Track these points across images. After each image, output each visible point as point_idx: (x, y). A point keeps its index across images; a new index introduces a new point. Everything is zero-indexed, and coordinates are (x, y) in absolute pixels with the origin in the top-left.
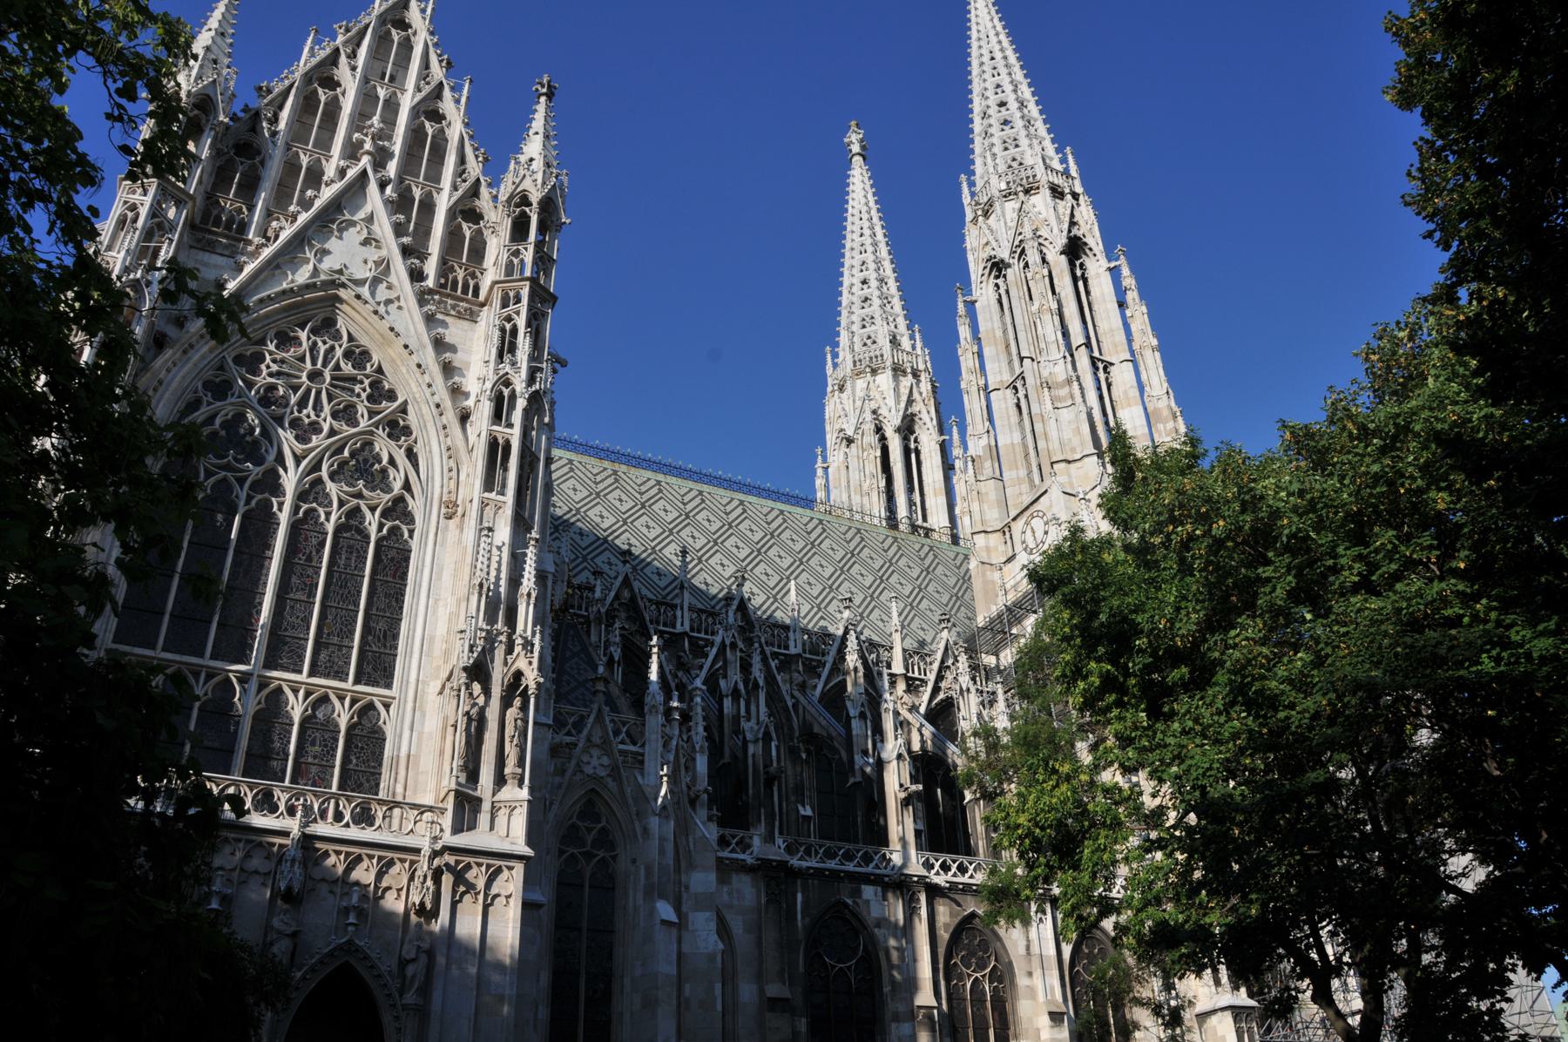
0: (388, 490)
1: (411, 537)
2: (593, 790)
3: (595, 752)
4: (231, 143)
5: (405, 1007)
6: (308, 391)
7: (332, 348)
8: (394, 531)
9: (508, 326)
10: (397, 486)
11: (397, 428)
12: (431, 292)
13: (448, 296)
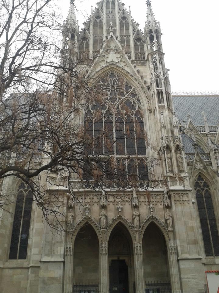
0: (135, 109)
1: (143, 119)
2: (200, 173)
3: (198, 163)
4: (81, 38)
5: (169, 231)
6: (112, 91)
8: (139, 118)
9: (154, 64)
10: (137, 108)
11: (134, 95)
12: (134, 61)
13: (138, 61)
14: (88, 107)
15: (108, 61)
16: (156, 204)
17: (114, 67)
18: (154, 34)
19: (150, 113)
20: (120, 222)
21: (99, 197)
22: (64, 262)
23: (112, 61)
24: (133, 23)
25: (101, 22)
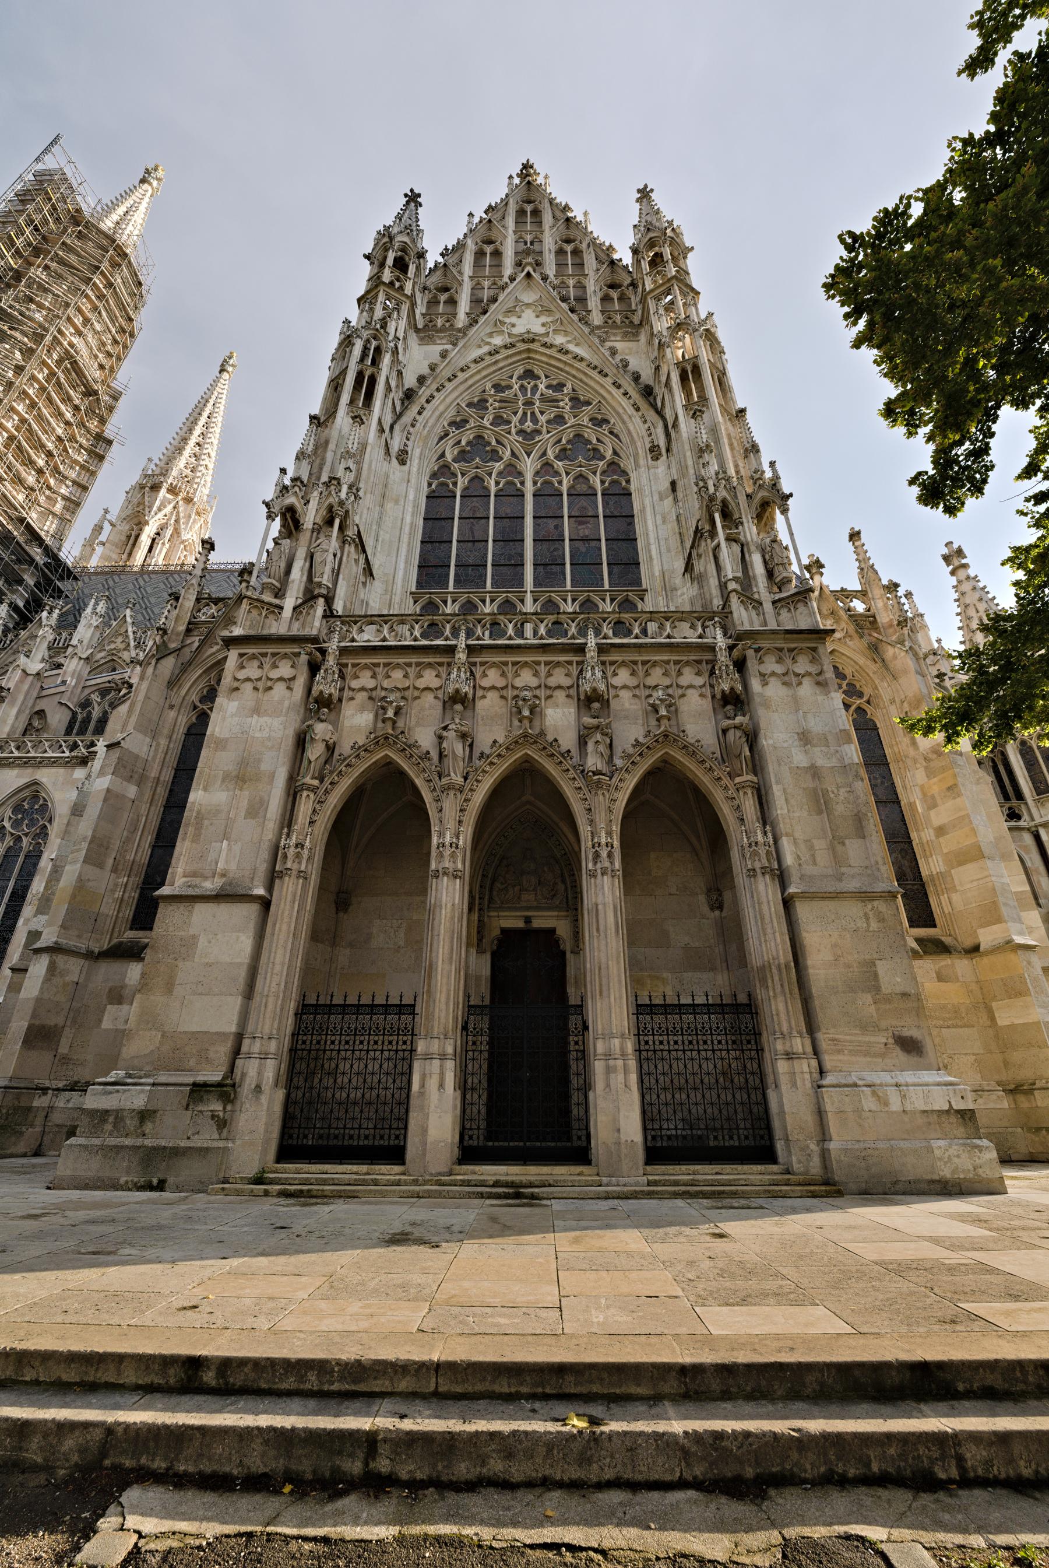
0: (604, 458)
7: (536, 386)
10: (609, 454)
12: (598, 327)
14: (443, 455)
15: (515, 331)
16: (683, 695)
17: (534, 346)
18: (659, 244)
19: (656, 458)
20: (527, 760)
21: (443, 670)
22: (266, 904)
23: (528, 332)
24: (594, 243)
25: (497, 254)
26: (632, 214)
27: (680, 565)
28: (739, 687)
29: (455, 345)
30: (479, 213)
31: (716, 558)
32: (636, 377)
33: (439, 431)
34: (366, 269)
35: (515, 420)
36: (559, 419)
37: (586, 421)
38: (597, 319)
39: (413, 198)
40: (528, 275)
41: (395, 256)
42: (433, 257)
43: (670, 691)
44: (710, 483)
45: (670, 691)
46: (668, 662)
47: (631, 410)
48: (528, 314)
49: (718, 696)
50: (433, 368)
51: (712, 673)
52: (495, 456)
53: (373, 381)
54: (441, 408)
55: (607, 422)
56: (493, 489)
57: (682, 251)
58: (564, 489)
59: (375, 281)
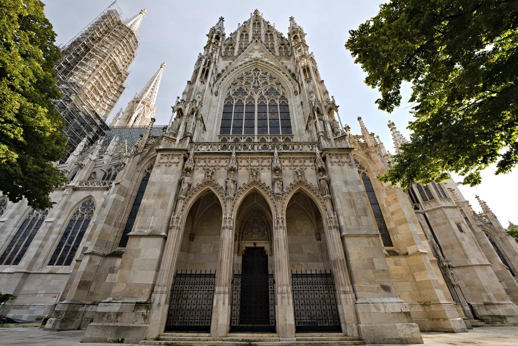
10: (281, 93)
14: (229, 93)
15: (252, 57)
18: (296, 33)
20: (255, 189)
21: (228, 160)
22: (165, 238)
24: (276, 32)
25: (247, 35)
26: (288, 24)
27: (304, 127)
28: (324, 166)
29: (234, 61)
30: (242, 24)
31: (316, 125)
32: (290, 71)
33: (228, 86)
34: (207, 39)
35: (252, 83)
36: (266, 83)
37: (274, 84)
38: (277, 54)
39: (222, 19)
40: (257, 41)
41: (216, 35)
42: (227, 36)
43: (302, 167)
44: (313, 103)
45: (302, 167)
46: (301, 158)
47: (288, 81)
48: (256, 52)
49: (317, 169)
50: (227, 67)
51: (315, 161)
52: (246, 94)
53: (208, 71)
54: (229, 79)
55: (281, 84)
56: (245, 104)
57: (303, 35)
58: (267, 104)
59: (210, 42)
